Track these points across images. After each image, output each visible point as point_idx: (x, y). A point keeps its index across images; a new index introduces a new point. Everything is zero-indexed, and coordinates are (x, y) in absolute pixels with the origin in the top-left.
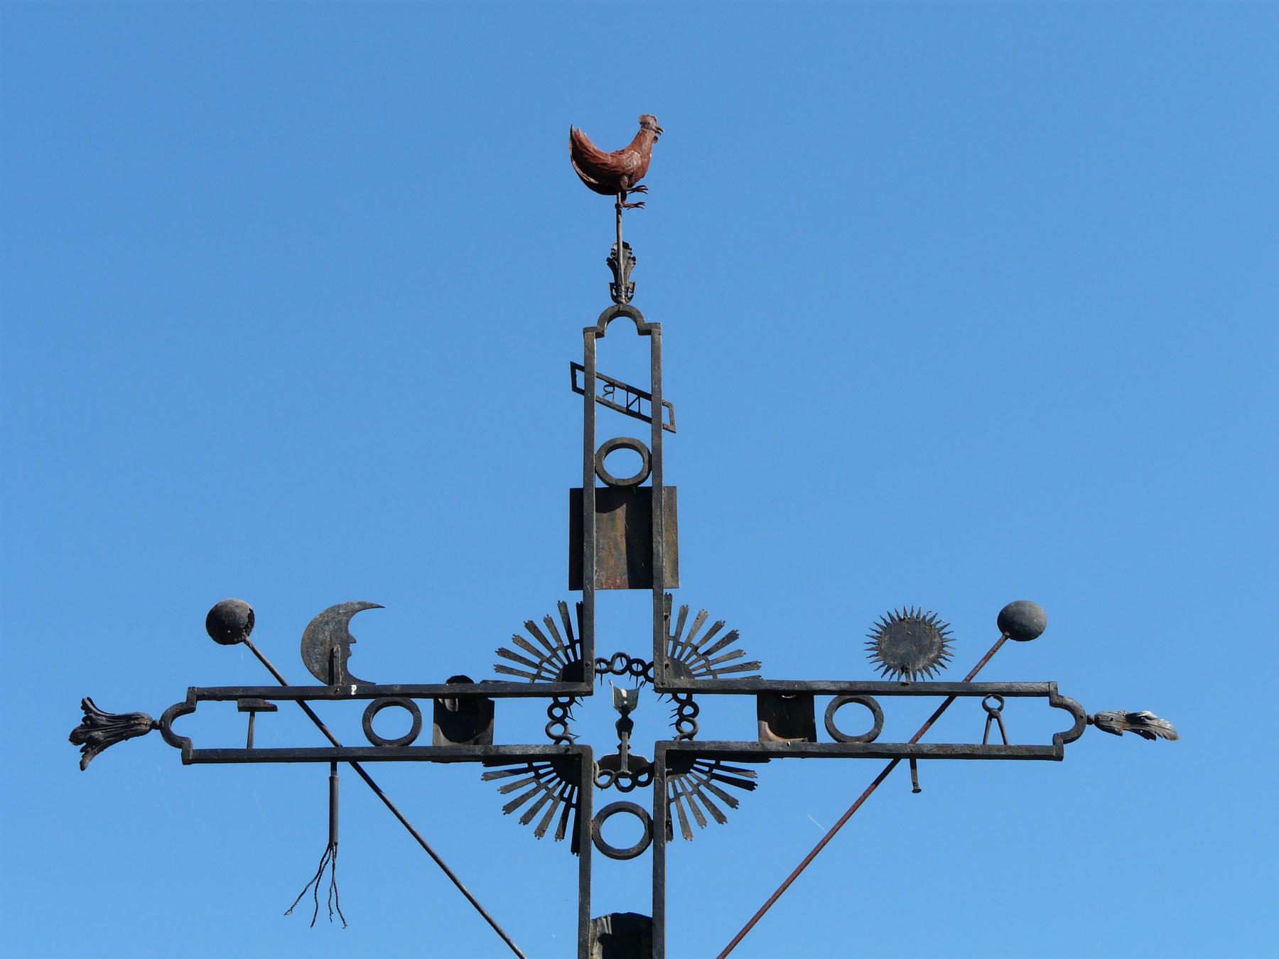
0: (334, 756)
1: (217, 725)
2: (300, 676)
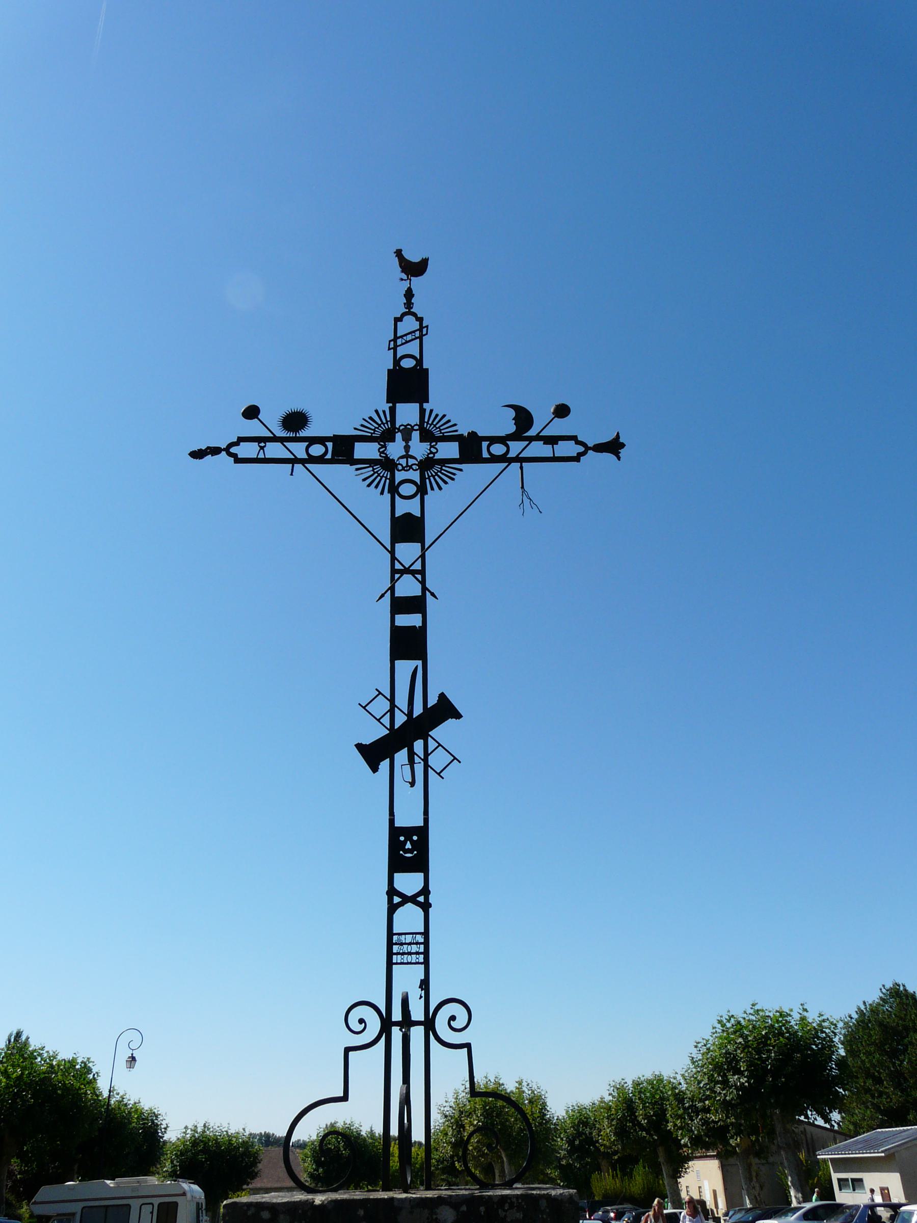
0: (294, 461)
1: (247, 450)
2: (280, 433)
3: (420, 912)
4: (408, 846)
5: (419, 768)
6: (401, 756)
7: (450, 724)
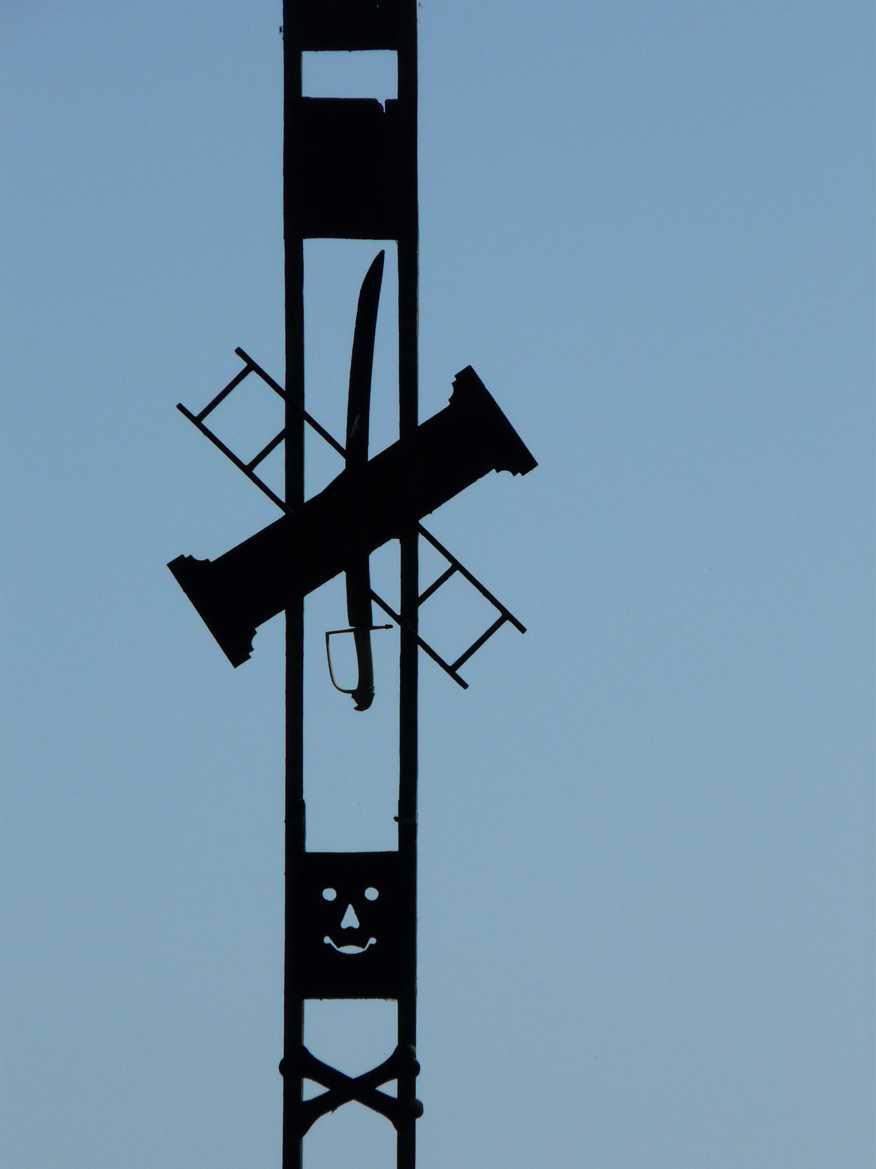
3: (384, 1130)
4: (350, 919)
5: (386, 644)
6: (326, 603)
7: (492, 490)
